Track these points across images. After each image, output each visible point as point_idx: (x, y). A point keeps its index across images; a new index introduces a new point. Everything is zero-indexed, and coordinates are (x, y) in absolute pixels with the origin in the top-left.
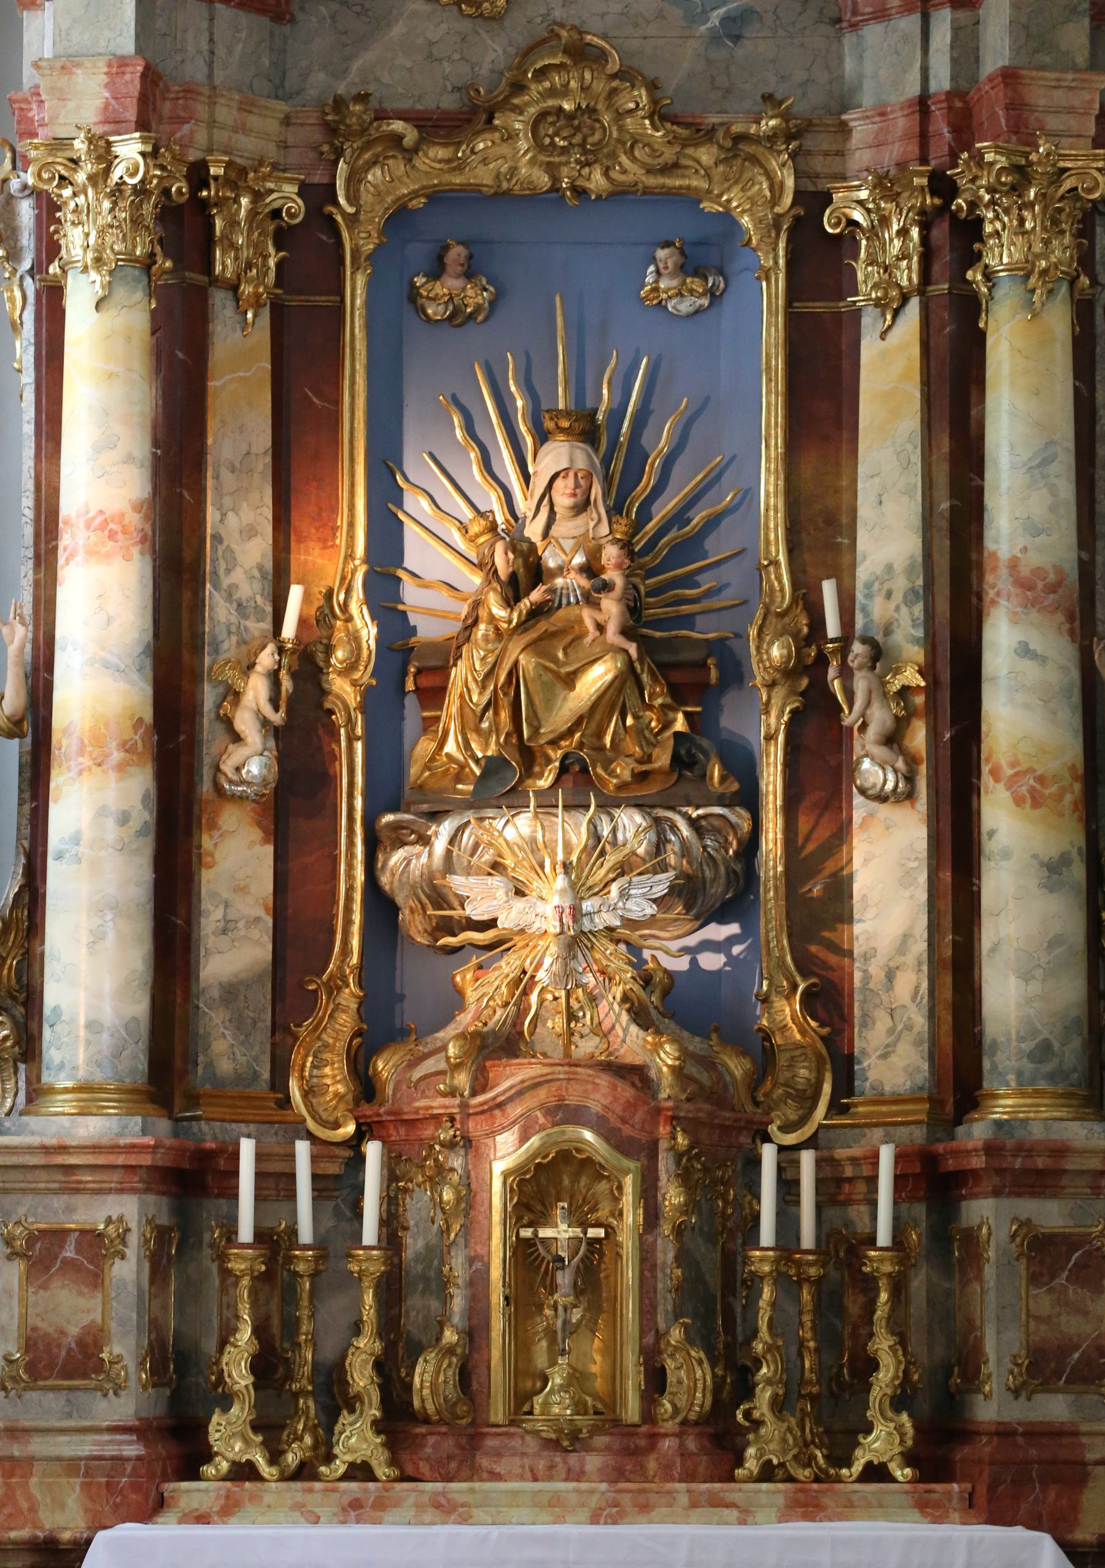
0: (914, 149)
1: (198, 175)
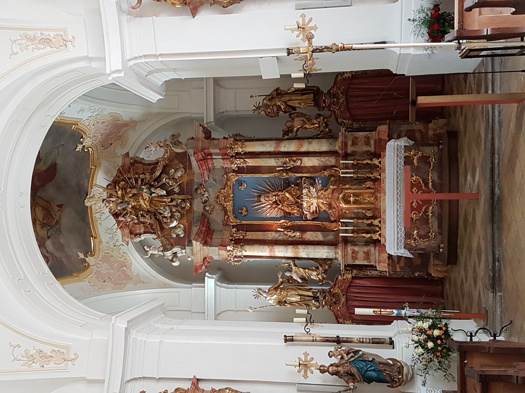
0: (228, 160)
1: (231, 240)
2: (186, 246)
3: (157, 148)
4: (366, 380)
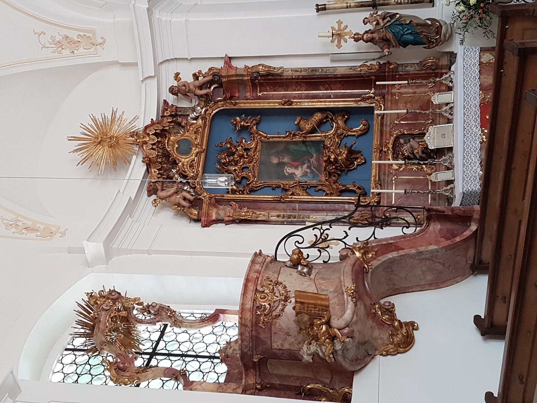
4: (402, 44)
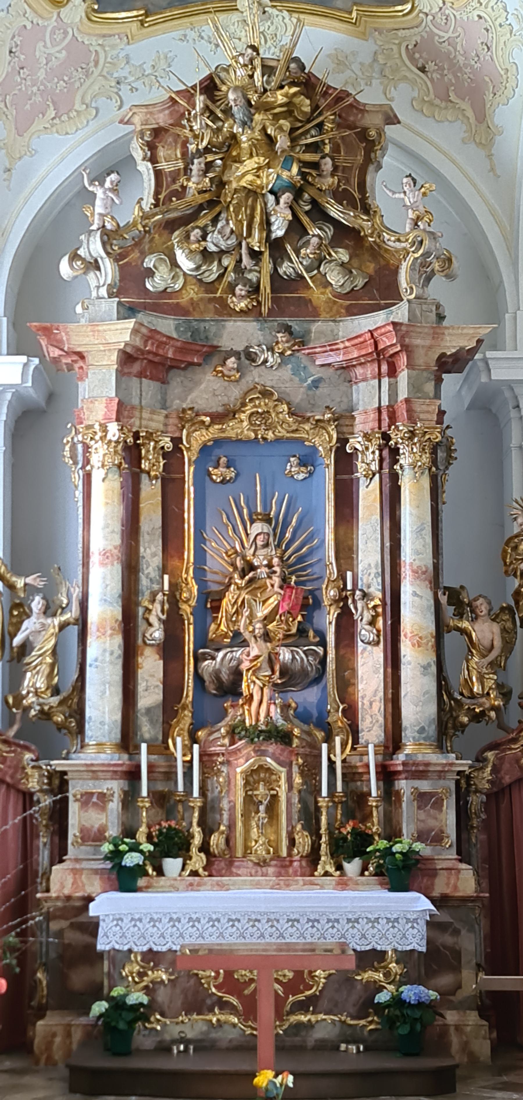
0: (377, 425)
1: (136, 436)
2: (117, 299)
3: (410, 211)
